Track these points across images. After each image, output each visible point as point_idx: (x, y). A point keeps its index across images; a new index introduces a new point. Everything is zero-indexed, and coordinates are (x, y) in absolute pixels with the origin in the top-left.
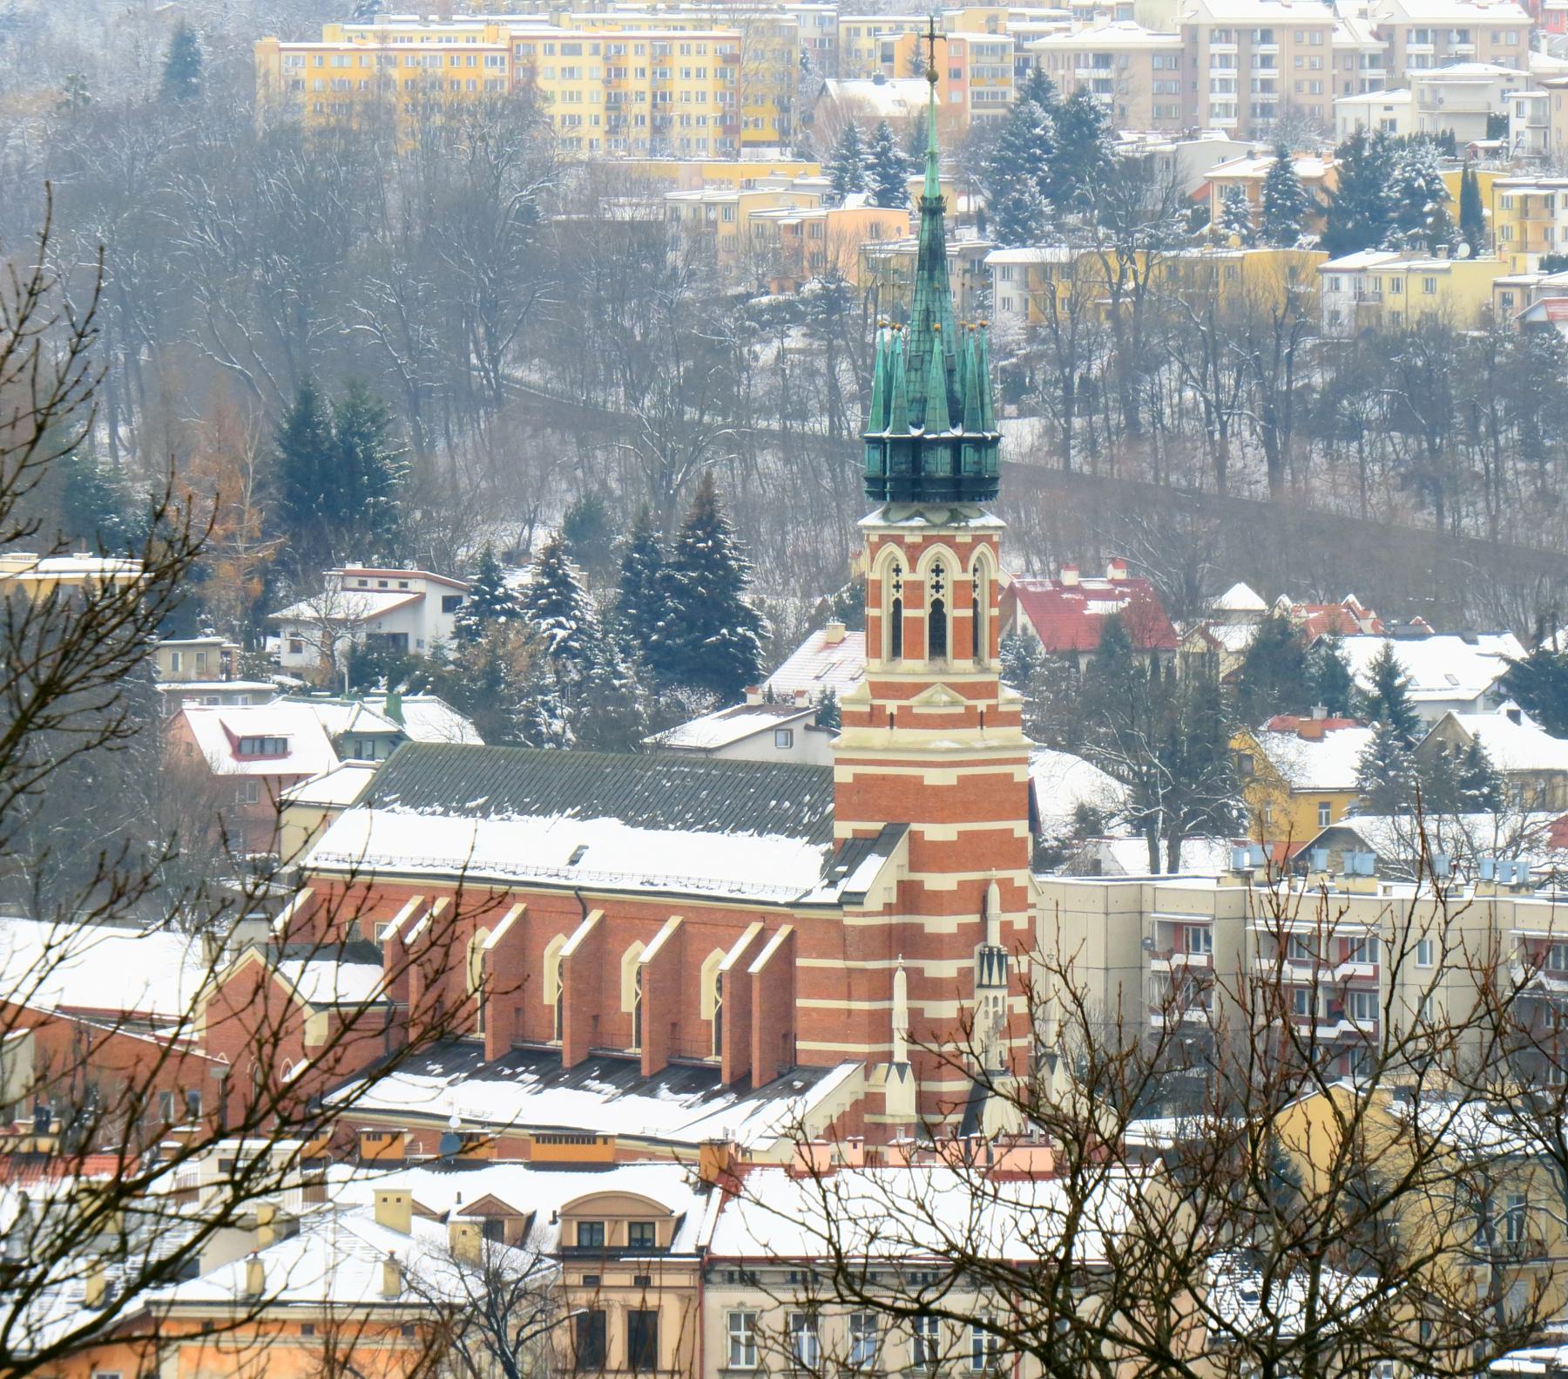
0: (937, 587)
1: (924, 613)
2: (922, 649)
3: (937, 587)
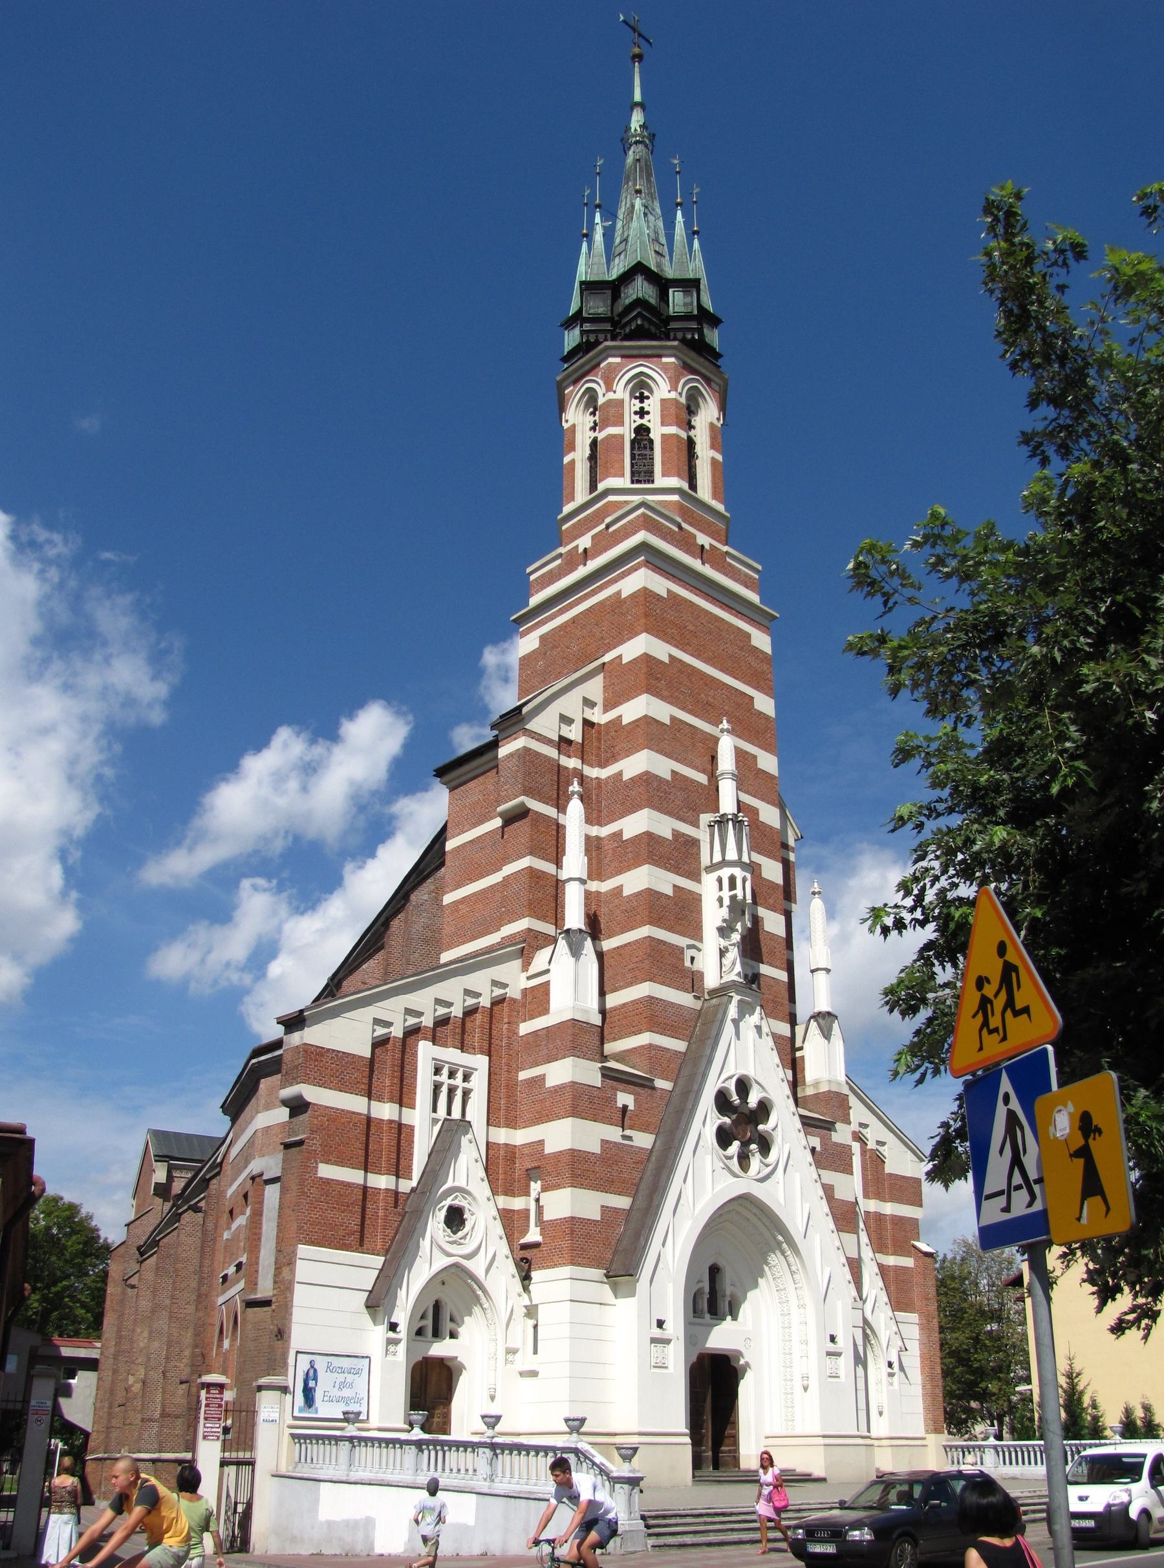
0: (642, 413)
1: (626, 432)
3: (642, 413)
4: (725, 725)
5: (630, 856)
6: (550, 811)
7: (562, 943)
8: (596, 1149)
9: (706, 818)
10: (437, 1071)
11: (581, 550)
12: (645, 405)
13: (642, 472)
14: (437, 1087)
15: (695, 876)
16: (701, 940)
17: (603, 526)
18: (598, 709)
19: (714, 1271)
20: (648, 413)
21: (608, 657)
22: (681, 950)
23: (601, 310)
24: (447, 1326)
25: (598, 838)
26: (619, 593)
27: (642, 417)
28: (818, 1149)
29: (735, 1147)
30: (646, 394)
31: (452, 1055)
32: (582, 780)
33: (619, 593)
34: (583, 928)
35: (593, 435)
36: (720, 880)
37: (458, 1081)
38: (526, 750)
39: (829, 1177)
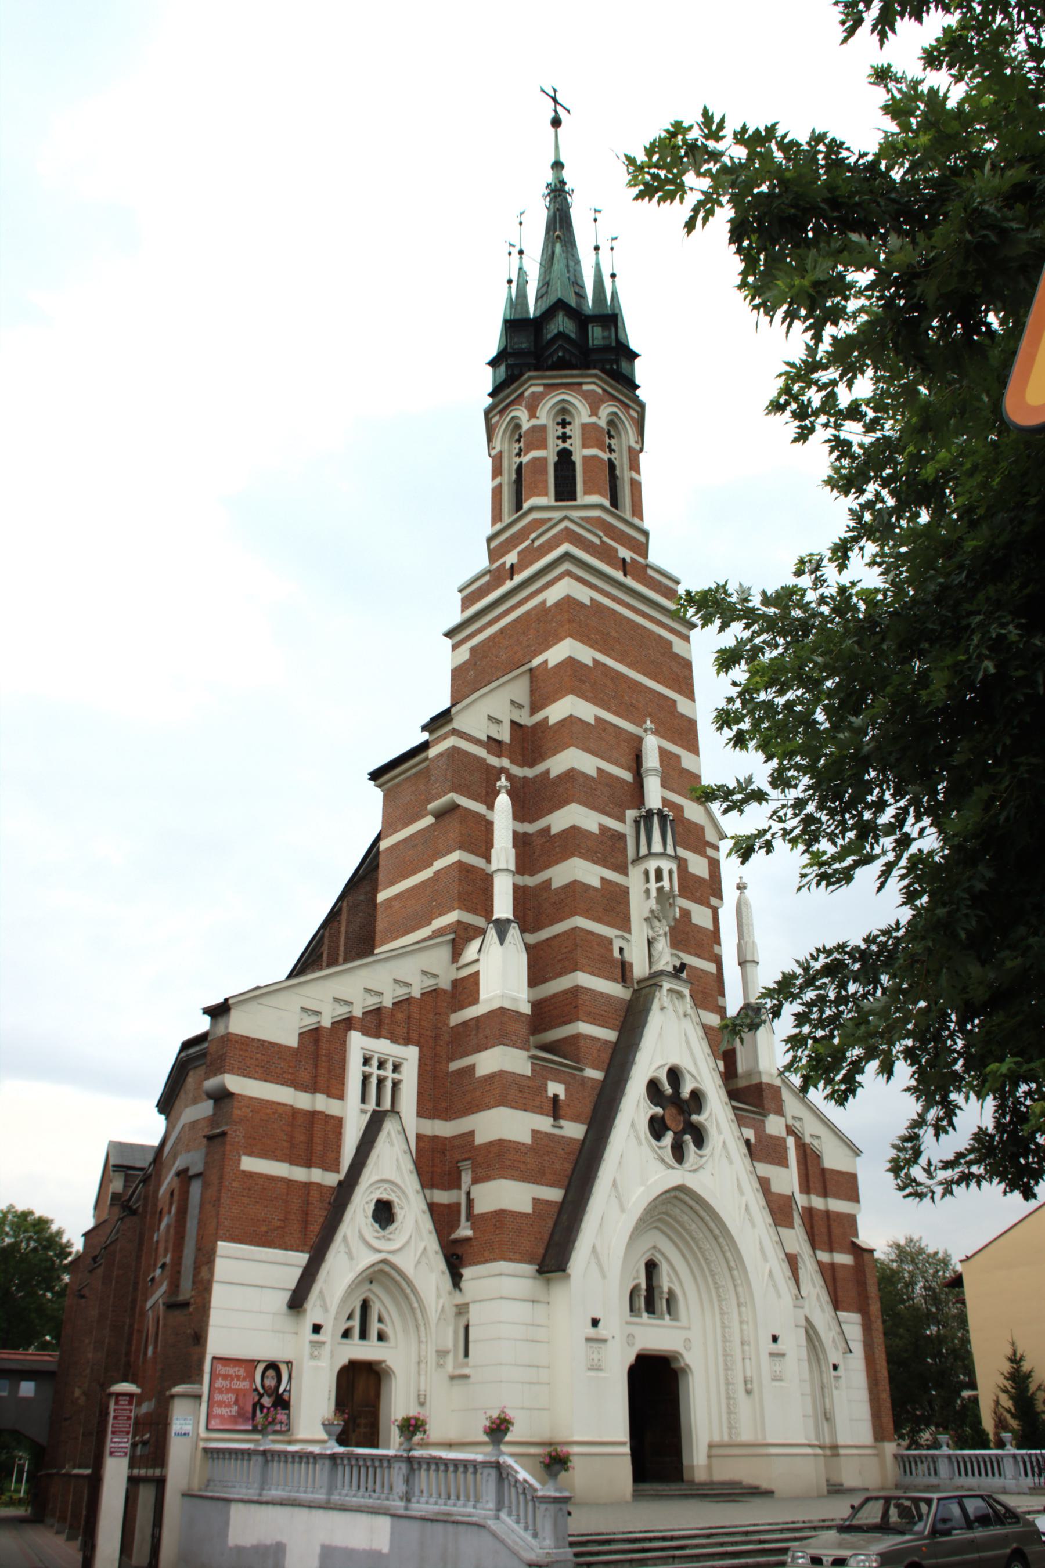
0: (564, 438)
1: (550, 454)
2: (546, 487)
3: (564, 438)
4: (649, 724)
5: (558, 850)
6: (479, 808)
7: (492, 933)
8: (527, 1139)
9: (631, 814)
10: (366, 1061)
11: (508, 566)
12: (568, 430)
13: (566, 491)
14: (366, 1078)
15: (623, 870)
16: (629, 931)
17: (528, 542)
18: (526, 711)
19: (651, 1267)
20: (570, 437)
21: (536, 662)
22: (610, 942)
23: (524, 346)
24: (374, 1327)
25: (525, 834)
26: (544, 602)
27: (564, 441)
28: (753, 1141)
29: (668, 1139)
30: (568, 420)
31: (383, 1046)
32: (510, 777)
33: (544, 602)
34: (511, 917)
35: (517, 460)
36: (647, 873)
37: (388, 1073)
38: (454, 749)
39: (765, 1169)
